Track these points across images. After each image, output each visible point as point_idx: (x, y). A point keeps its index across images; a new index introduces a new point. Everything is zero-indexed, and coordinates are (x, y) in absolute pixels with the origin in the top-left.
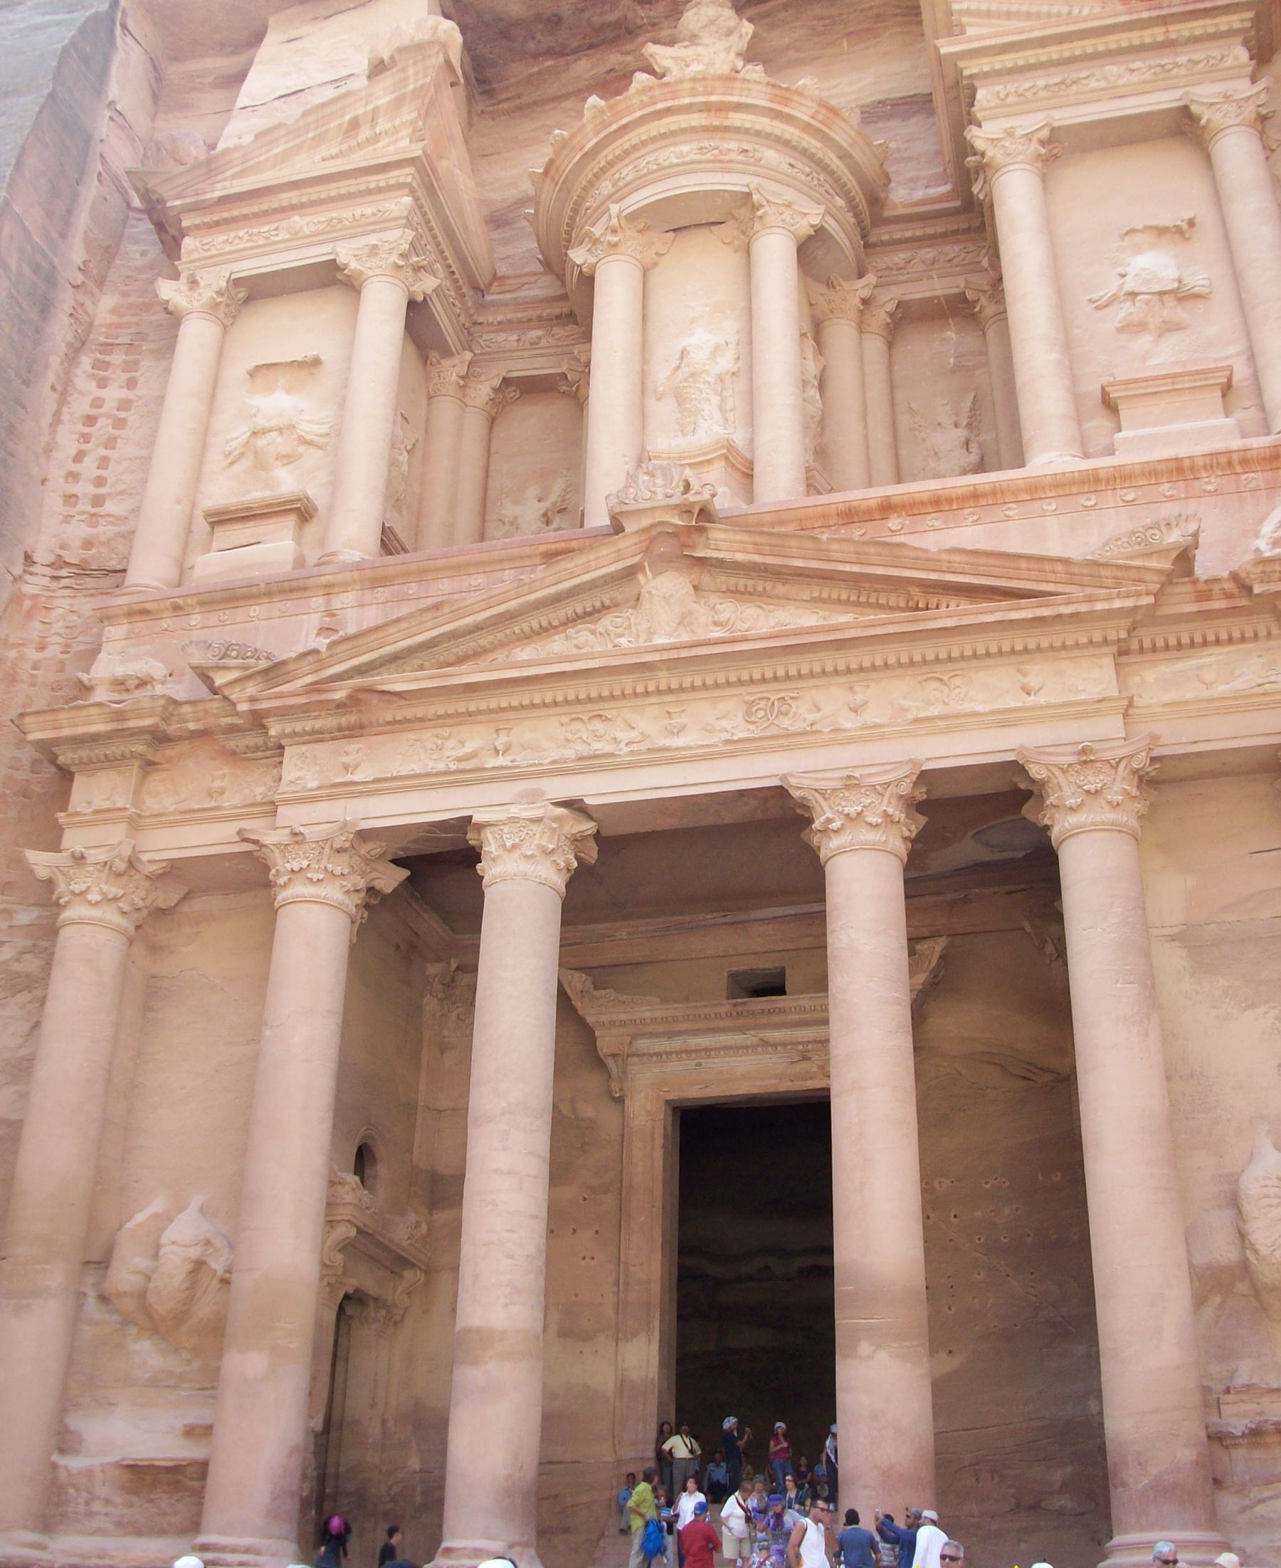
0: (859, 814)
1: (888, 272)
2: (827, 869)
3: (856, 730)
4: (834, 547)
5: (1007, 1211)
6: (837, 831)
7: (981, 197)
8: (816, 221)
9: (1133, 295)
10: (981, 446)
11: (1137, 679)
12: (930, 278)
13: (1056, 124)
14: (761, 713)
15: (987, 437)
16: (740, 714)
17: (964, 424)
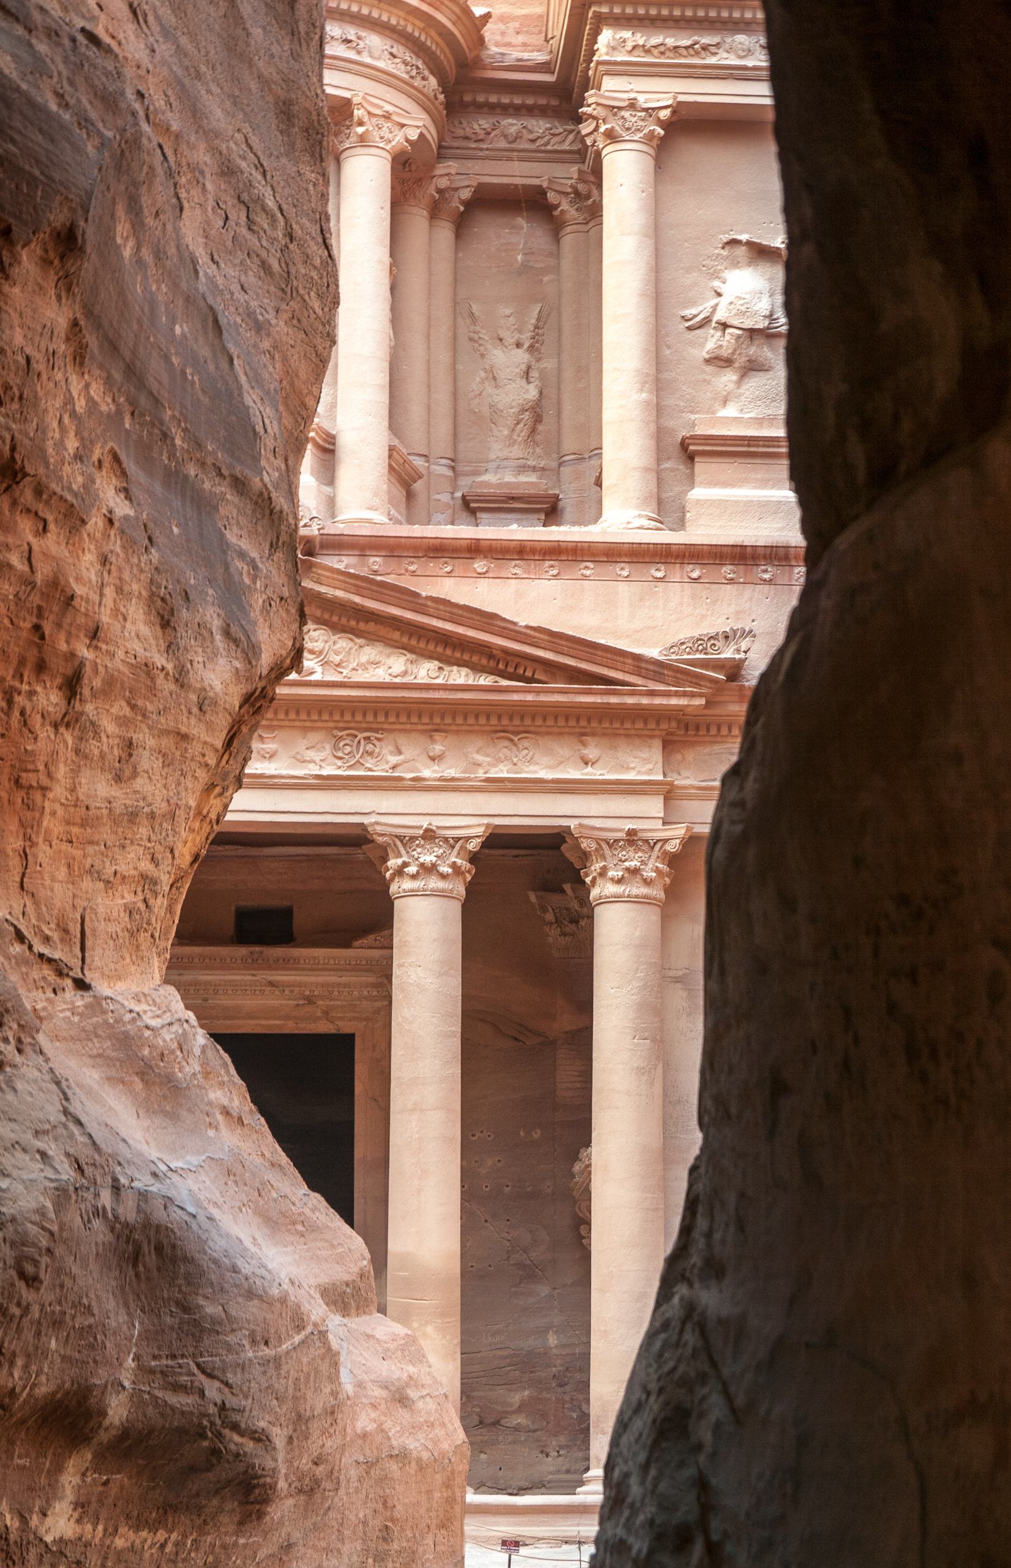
0: (434, 866)
1: (463, 144)
2: (397, 903)
3: (434, 780)
4: (429, 603)
5: (490, 1162)
6: (414, 877)
7: (589, 141)
8: (414, 135)
9: (724, 326)
10: (543, 377)
11: (679, 757)
12: (510, 159)
13: (681, 98)
14: (348, 749)
15: (549, 364)
16: (328, 747)
17: (526, 346)
